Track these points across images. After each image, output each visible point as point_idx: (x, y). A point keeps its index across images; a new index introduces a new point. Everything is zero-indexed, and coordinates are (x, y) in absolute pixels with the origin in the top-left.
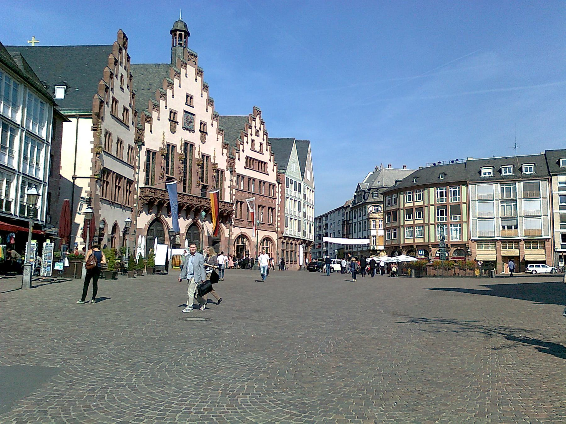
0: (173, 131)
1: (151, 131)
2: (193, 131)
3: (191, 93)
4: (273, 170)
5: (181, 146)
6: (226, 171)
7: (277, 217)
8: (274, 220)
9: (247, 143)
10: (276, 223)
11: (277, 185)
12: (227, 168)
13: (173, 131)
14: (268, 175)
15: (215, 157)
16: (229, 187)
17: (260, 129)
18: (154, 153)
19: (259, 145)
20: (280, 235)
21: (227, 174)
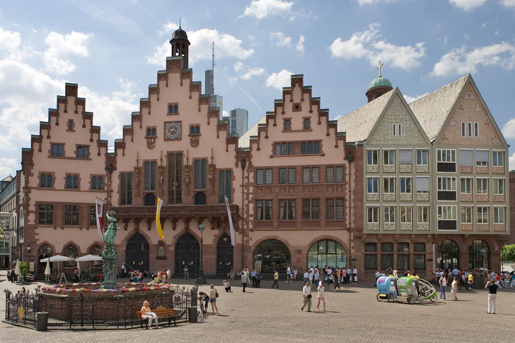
0: (151, 145)
1: (124, 155)
2: (179, 139)
3: (173, 101)
5: (161, 160)
7: (347, 211)
9: (275, 125)
10: (347, 217)
11: (347, 165)
12: (237, 166)
14: (324, 155)
15: (212, 158)
16: (241, 186)
17: (302, 100)
18: (130, 174)
19: (302, 120)
20: (357, 233)
21: (238, 173)
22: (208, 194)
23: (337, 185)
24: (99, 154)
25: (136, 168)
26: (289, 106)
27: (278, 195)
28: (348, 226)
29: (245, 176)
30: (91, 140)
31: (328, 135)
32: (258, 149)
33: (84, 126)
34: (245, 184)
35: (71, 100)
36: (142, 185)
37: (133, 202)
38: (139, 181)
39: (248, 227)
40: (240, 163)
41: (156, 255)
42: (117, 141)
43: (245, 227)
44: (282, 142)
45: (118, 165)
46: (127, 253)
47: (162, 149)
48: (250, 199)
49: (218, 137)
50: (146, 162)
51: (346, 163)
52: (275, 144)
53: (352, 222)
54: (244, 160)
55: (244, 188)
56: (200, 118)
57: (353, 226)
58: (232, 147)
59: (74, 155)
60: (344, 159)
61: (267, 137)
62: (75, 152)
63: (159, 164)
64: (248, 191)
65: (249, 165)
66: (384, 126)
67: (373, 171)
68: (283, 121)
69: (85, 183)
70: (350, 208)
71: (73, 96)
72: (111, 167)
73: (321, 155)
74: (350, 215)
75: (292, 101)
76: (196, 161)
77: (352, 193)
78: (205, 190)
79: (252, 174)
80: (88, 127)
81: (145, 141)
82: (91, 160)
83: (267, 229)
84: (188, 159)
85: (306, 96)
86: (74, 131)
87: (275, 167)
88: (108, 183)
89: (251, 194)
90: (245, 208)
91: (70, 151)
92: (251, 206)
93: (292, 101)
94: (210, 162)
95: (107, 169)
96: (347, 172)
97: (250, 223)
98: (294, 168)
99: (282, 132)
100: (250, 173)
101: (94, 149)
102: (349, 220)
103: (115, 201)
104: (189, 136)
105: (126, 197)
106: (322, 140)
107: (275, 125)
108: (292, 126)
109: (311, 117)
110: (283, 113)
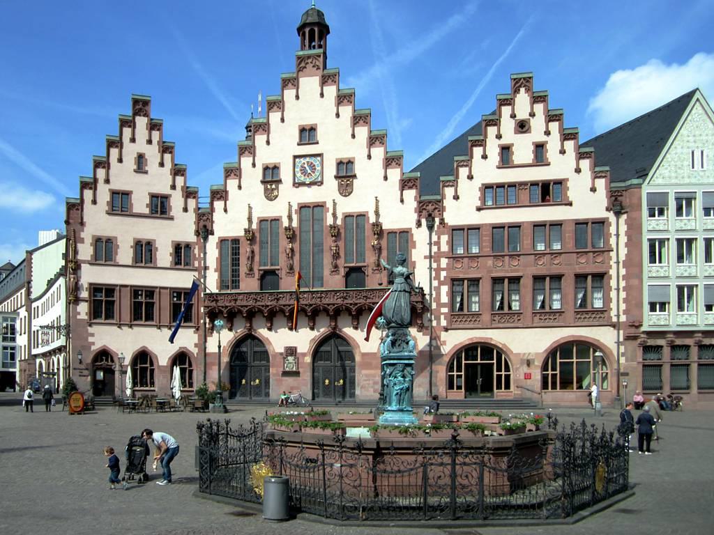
1: (226, 211)
4: (593, 190)
5: (290, 218)
6: (415, 231)
7: (613, 294)
8: (607, 300)
9: (485, 157)
10: (613, 305)
12: (419, 224)
13: (270, 196)
14: (571, 204)
15: (377, 213)
16: (425, 257)
17: (532, 115)
18: (236, 241)
19: (532, 148)
20: (632, 331)
21: (421, 236)
22: (369, 271)
23: (594, 252)
24: (185, 210)
25: (247, 231)
26: (507, 125)
27: (491, 272)
28: (615, 319)
29: (433, 242)
30: (173, 187)
31: (578, 171)
32: (456, 197)
33: (162, 164)
34: (433, 254)
35: (141, 122)
36: (257, 258)
37: (242, 285)
38: (253, 252)
39: (439, 323)
40: (424, 221)
41: (282, 369)
42: (215, 188)
43: (434, 323)
44: (496, 184)
45: (215, 227)
46: (231, 366)
47: (290, 197)
48: (442, 279)
49: (386, 178)
50: (262, 221)
51: (611, 216)
52: (487, 187)
53: (621, 313)
54: (430, 215)
55: (432, 260)
56: (356, 148)
57: (623, 318)
58: (410, 194)
59: (147, 211)
60: (608, 209)
61: (470, 177)
62: (147, 205)
63: (286, 223)
64: (439, 265)
65: (441, 223)
66: (676, 154)
67: (657, 228)
68: (498, 150)
69: (164, 256)
70: (618, 289)
71: (144, 116)
72: (204, 231)
73: (566, 205)
74: (618, 301)
75: (513, 116)
76: (347, 216)
77: (621, 265)
78: (365, 264)
79: (445, 238)
80: (168, 165)
81: (262, 187)
82: (172, 219)
83: (471, 326)
84: (334, 215)
85: (539, 108)
86: (146, 172)
87: (486, 224)
88: (199, 255)
89: (443, 269)
90: (434, 293)
91: (140, 203)
92: (445, 289)
93: (513, 116)
94: (372, 219)
95: (197, 233)
96: (613, 230)
97: (442, 317)
98: (517, 226)
99: (498, 168)
100: (442, 237)
101: (177, 200)
102: (618, 310)
103: (212, 284)
104: (336, 177)
105: (230, 277)
106: (567, 180)
107: (485, 157)
108: (514, 158)
109: (547, 142)
110: (499, 137)
